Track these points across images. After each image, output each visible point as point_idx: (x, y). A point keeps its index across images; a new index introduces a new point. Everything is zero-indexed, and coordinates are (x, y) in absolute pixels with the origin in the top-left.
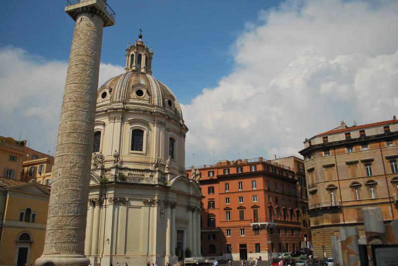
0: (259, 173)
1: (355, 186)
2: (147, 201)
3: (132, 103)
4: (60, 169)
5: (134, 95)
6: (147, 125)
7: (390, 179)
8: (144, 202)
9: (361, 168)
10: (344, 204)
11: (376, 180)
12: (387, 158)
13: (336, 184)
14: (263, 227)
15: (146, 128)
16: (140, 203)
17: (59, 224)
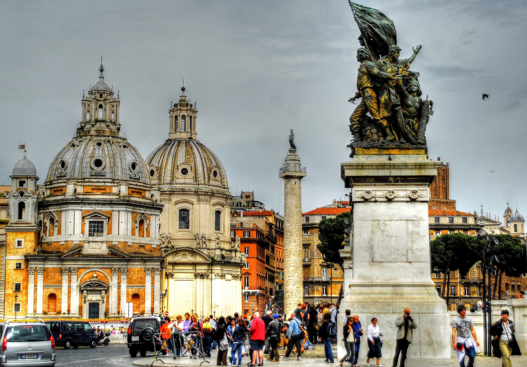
3: (213, 186)
10: (333, 280)
14: (254, 294)
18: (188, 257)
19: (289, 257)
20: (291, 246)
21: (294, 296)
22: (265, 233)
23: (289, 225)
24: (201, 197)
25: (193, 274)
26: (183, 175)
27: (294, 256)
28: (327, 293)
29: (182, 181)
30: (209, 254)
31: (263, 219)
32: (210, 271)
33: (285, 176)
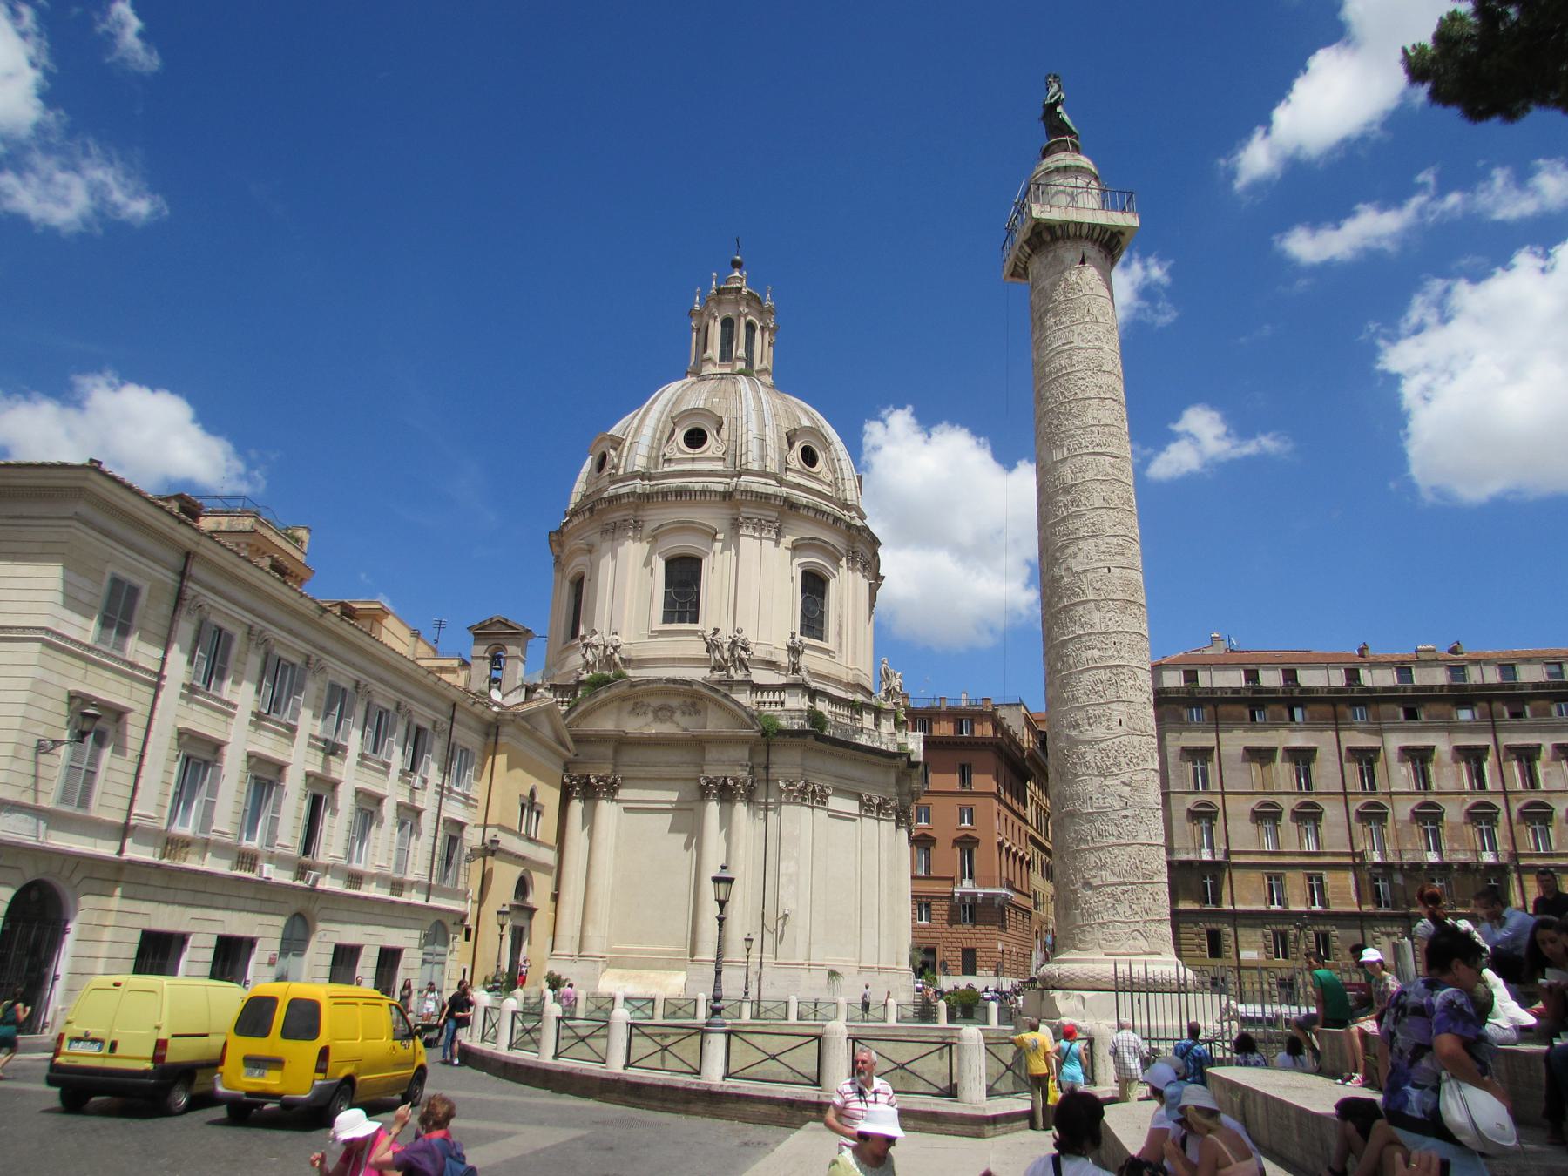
0: (977, 743)
1: (1266, 815)
2: (870, 800)
3: (797, 486)
4: (1121, 707)
5: (795, 457)
6: (837, 566)
7: (1356, 805)
8: (862, 804)
9: (1283, 773)
10: (1234, 859)
11: (1323, 802)
12: (1349, 749)
13: (1217, 800)
15: (836, 573)
16: (852, 806)
17: (1144, 866)
18: (678, 716)
19: (1071, 619)
20: (1080, 556)
21: (1112, 840)
22: (1026, 745)
23: (1057, 456)
24: (746, 511)
25: (693, 785)
26: (690, 450)
27: (1098, 608)
28: (1217, 900)
29: (688, 467)
30: (762, 708)
31: (1020, 710)
32: (761, 772)
33: (1028, 242)
